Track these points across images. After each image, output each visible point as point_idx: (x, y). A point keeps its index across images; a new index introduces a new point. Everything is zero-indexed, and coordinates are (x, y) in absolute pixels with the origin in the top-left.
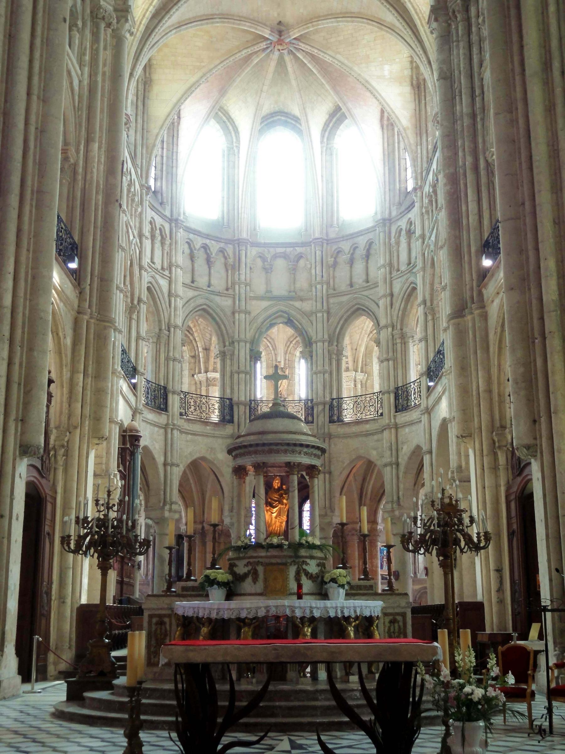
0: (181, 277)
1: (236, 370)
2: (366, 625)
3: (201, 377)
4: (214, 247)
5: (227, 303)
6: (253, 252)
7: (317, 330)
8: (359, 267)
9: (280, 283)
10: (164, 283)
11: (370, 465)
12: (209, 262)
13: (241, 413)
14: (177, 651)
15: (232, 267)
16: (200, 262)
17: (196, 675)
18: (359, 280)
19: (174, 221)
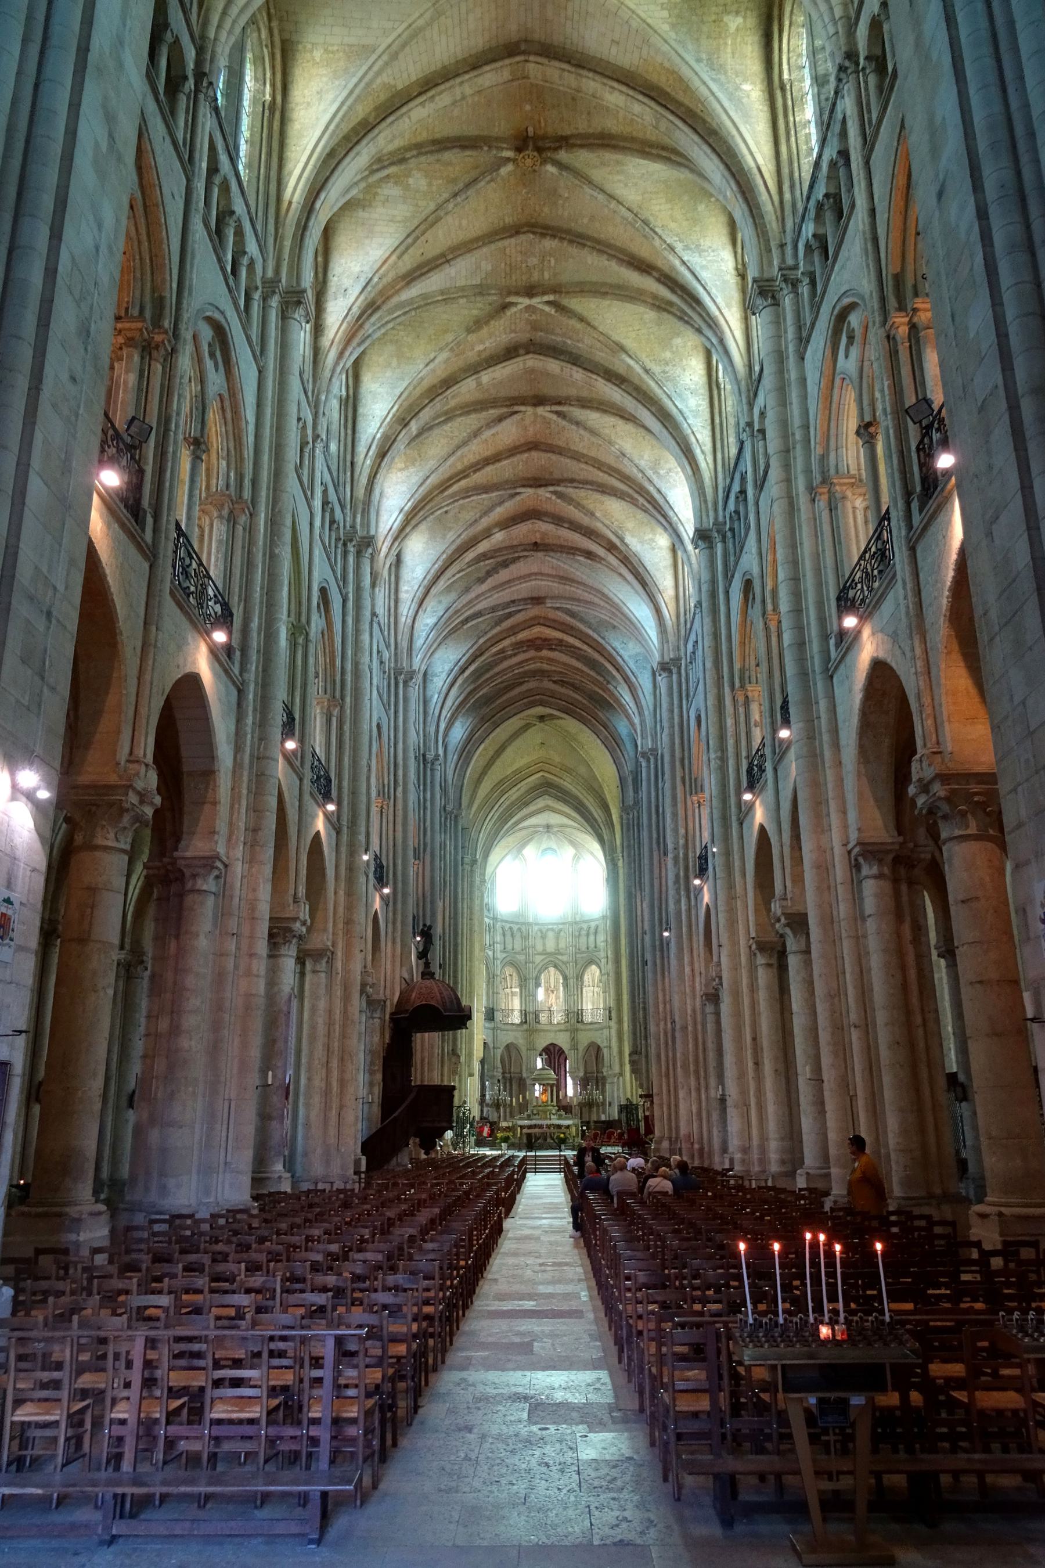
0: (499, 947)
1: (528, 996)
2: (568, 1127)
3: (508, 990)
4: (515, 927)
5: (522, 958)
6: (536, 928)
7: (570, 972)
8: (592, 938)
9: (551, 946)
10: (490, 953)
11: (599, 1049)
12: (512, 935)
13: (531, 1018)
14: (525, 1131)
15: (525, 937)
16: (509, 938)
17: (529, 1135)
18: (592, 945)
19: (495, 919)
